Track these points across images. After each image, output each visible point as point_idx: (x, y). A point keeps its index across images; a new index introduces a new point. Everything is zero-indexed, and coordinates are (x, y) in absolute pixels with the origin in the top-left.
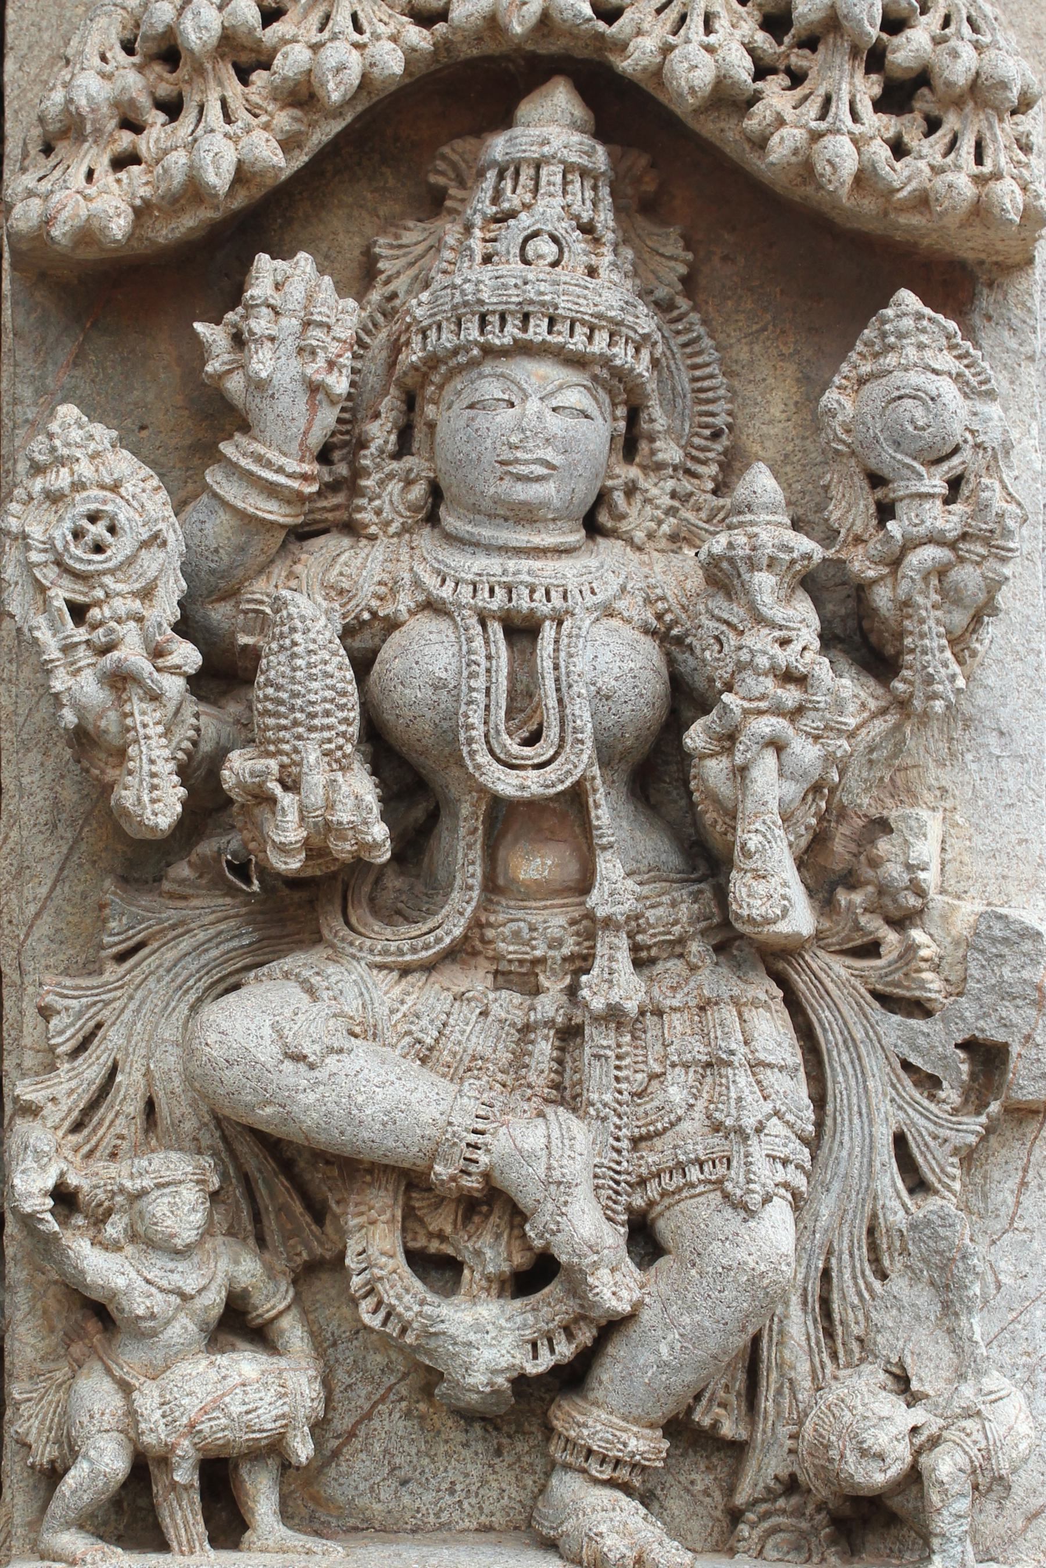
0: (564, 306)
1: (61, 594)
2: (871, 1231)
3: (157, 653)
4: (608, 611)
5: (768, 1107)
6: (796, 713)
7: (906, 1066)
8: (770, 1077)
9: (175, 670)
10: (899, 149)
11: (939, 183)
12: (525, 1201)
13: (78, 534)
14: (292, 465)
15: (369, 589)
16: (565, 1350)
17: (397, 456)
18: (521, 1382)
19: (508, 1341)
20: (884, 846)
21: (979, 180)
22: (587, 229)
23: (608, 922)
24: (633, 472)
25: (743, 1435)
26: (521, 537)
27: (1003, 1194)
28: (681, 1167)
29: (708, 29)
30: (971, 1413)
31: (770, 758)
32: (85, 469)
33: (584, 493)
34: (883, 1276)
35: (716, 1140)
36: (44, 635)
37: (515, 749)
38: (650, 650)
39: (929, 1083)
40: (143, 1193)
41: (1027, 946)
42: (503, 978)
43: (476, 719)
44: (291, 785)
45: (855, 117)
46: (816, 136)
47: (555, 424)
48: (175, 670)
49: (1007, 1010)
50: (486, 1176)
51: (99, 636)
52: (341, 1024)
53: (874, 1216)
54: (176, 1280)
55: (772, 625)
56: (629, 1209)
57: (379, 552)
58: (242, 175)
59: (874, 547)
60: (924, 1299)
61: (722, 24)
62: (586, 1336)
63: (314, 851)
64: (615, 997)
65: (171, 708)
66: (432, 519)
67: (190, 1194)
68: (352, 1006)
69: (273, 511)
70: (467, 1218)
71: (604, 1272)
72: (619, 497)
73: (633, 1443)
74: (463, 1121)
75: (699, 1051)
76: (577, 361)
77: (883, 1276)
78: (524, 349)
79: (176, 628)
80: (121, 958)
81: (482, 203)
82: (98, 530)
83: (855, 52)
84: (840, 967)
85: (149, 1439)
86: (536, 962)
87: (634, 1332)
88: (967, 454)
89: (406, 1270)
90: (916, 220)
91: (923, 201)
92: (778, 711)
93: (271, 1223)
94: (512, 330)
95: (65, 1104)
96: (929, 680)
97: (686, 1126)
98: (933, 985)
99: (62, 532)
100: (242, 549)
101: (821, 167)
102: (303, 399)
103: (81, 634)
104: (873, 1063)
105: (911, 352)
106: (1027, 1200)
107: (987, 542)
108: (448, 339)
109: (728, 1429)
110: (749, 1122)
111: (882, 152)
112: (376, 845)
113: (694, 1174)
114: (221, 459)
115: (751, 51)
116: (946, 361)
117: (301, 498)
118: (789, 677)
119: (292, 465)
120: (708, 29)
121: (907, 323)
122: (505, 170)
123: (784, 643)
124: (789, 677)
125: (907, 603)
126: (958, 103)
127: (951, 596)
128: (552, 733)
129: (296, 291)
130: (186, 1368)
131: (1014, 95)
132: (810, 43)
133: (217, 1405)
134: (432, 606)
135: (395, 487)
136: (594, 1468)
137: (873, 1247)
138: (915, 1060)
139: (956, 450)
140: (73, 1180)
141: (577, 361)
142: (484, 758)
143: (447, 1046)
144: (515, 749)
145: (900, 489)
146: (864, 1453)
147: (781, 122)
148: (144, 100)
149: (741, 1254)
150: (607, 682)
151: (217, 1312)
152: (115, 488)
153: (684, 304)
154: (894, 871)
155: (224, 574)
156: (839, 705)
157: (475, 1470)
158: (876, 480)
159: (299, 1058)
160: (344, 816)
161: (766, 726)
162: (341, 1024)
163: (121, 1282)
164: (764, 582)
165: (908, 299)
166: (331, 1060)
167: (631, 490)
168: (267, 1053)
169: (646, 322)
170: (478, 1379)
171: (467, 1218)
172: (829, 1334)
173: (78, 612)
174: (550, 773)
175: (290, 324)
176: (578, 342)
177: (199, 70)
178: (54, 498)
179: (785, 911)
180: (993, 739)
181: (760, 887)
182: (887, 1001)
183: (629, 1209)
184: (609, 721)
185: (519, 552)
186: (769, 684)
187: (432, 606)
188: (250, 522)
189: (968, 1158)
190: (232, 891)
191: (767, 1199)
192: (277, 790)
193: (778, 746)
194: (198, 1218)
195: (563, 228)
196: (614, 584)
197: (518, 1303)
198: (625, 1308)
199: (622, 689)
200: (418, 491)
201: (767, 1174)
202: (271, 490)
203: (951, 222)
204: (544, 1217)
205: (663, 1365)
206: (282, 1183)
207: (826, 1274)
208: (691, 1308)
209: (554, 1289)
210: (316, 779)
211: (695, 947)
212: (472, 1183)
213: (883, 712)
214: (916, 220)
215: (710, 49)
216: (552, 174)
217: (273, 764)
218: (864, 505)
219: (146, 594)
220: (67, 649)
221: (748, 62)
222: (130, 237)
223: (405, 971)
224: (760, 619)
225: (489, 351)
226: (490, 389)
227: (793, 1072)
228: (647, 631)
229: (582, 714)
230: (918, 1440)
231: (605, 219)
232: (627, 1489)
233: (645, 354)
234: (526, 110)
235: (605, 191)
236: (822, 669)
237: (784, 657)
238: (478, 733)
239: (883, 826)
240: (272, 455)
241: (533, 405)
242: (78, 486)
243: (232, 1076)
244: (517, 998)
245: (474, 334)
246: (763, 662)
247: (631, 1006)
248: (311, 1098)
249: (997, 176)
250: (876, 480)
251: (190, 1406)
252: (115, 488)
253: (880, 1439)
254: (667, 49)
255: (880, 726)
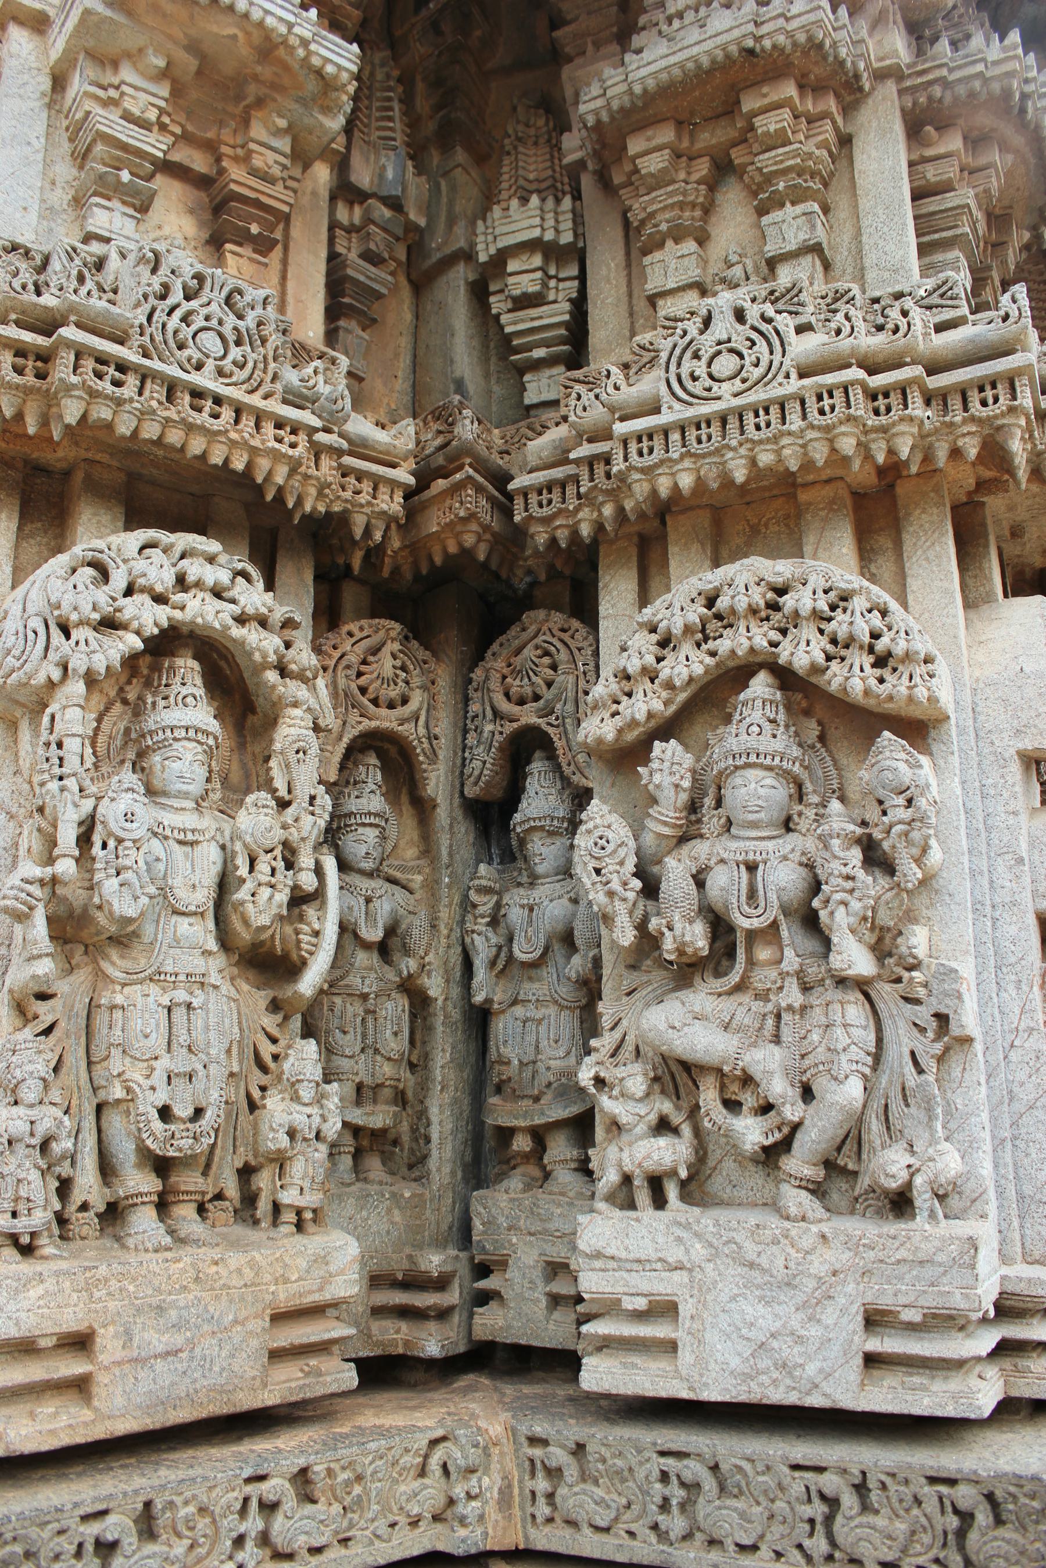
0: (762, 749)
1: (592, 864)
2: (903, 1089)
3: (625, 884)
4: (785, 858)
5: (849, 1041)
6: (852, 891)
7: (915, 1024)
8: (852, 1030)
9: (632, 889)
10: (881, 681)
11: (894, 692)
12: (758, 1079)
13: (596, 844)
14: (672, 814)
15: (703, 857)
16: (778, 1136)
17: (716, 809)
18: (765, 1149)
19: (758, 1132)
20: (899, 940)
21: (910, 688)
22: (773, 721)
23: (788, 973)
24: (800, 807)
25: (856, 1169)
26: (754, 833)
27: (957, 1072)
28: (816, 1065)
29: (808, 645)
30: (932, 1159)
31: (842, 908)
32: (598, 821)
33: (778, 816)
34: (907, 1105)
35: (829, 1054)
36: (585, 880)
37: (748, 910)
38: (803, 872)
39: (923, 1030)
40: (623, 1079)
41: (953, 975)
42: (757, 997)
43: (734, 901)
44: (671, 929)
45: (862, 670)
46: (847, 678)
47: (762, 792)
48: (632, 889)
49: (948, 1001)
50: (743, 1070)
51: (604, 879)
52: (690, 1015)
53: (903, 1084)
54: (637, 1110)
55: (840, 858)
56: (801, 1082)
57: (708, 843)
58: (650, 715)
59: (880, 828)
60: (922, 1115)
61: (812, 644)
62: (786, 1130)
63: (681, 952)
64: (790, 1001)
65: (631, 903)
66: (729, 830)
67: (640, 1079)
68: (697, 1008)
69: (667, 831)
70: (744, 1086)
71: (788, 1106)
72: (795, 817)
73: (806, 1172)
74: (732, 1050)
75: (823, 1020)
76: (769, 768)
77: (907, 1105)
78: (748, 766)
79: (635, 875)
80: (629, 994)
81: (737, 717)
82: (603, 842)
83: (861, 647)
84: (888, 987)
85: (625, 1169)
86: (769, 990)
87: (802, 1129)
88: (912, 789)
89: (720, 1106)
90: (891, 705)
91: (891, 698)
92: (844, 891)
93: (682, 1090)
94: (744, 759)
95: (608, 1047)
96: (905, 875)
97: (819, 1049)
98: (921, 992)
99: (591, 843)
100: (659, 846)
101: (849, 689)
102: (673, 790)
103: (599, 879)
104: (901, 1024)
105: (888, 754)
106: (966, 1075)
107: (921, 821)
108: (723, 765)
109: (851, 1166)
110: (840, 1047)
111: (873, 682)
112: (700, 949)
113: (821, 1067)
114: (650, 815)
115: (825, 652)
116: (903, 756)
117: (681, 826)
118: (849, 878)
119: (672, 814)
120: (808, 645)
121: (886, 743)
122: (745, 704)
123: (845, 865)
124: (849, 878)
125: (894, 847)
126: (903, 661)
127: (910, 843)
128: (762, 904)
129: (669, 753)
130: (641, 1143)
131: (922, 656)
132: (847, 646)
133: (648, 1156)
134: (722, 861)
135: (715, 820)
136: (793, 1181)
137: (904, 1096)
138: (918, 1022)
139: (908, 788)
140: (602, 1074)
141: (769, 768)
142: (737, 915)
143: (734, 1023)
144: (748, 910)
145: (887, 804)
146: (887, 1175)
147: (835, 675)
148: (619, 693)
149: (837, 1098)
150: (783, 884)
151: (654, 1123)
152: (609, 827)
153: (818, 745)
154: (903, 949)
155: (654, 855)
156: (867, 887)
157: (760, 1182)
158: (881, 802)
159: (674, 1028)
160: (687, 938)
161: (838, 897)
162: (690, 1015)
163: (617, 1111)
164: (835, 843)
165: (886, 734)
166: (686, 1028)
167: (800, 814)
168: (663, 1026)
169: (796, 752)
170: (748, 1147)
171: (744, 1086)
172: (888, 1128)
173: (598, 871)
174: (761, 919)
175: (667, 764)
176: (768, 761)
177: (636, 681)
178: (589, 832)
179: (850, 967)
180: (947, 897)
181: (839, 957)
182: (907, 999)
183: (801, 1082)
184: (786, 898)
185: (748, 838)
186: (840, 880)
187: (722, 861)
188: (659, 835)
189: (940, 1059)
190: (667, 969)
191: (847, 1077)
192: (665, 930)
193: (845, 904)
194: (644, 1087)
195: (761, 722)
196: (789, 847)
197: (760, 1118)
198: (796, 1119)
199: (789, 886)
200: (723, 820)
201: (846, 1067)
202: (665, 824)
203: (903, 704)
204: (763, 1085)
205: (813, 1141)
206: (685, 1075)
207: (886, 1106)
208: (821, 1119)
209: (773, 1113)
210: (678, 926)
211: (828, 982)
212: (738, 1073)
213: (892, 889)
214: (891, 705)
215: (807, 652)
216: (759, 703)
217: (664, 921)
218: (878, 810)
219: (621, 863)
220: (593, 884)
221: (823, 655)
222: (617, 740)
223: (720, 995)
224: (835, 857)
225: (737, 768)
226: (738, 781)
227: (865, 1028)
228: (801, 864)
229: (773, 897)
230: (912, 1170)
231: (781, 717)
232: (806, 1189)
233: (797, 764)
234: (752, 682)
235: (781, 707)
236: (860, 874)
237: (845, 871)
238: (735, 905)
239: (900, 933)
240: (664, 811)
241: (753, 785)
242: (596, 827)
243: (651, 1035)
244: (762, 1004)
245: (731, 762)
246: (836, 872)
247: (797, 1005)
248: (678, 1042)
249: (916, 686)
250: (881, 802)
251: (639, 1156)
252: (609, 827)
253: (893, 1169)
254: (792, 654)
255: (890, 894)
